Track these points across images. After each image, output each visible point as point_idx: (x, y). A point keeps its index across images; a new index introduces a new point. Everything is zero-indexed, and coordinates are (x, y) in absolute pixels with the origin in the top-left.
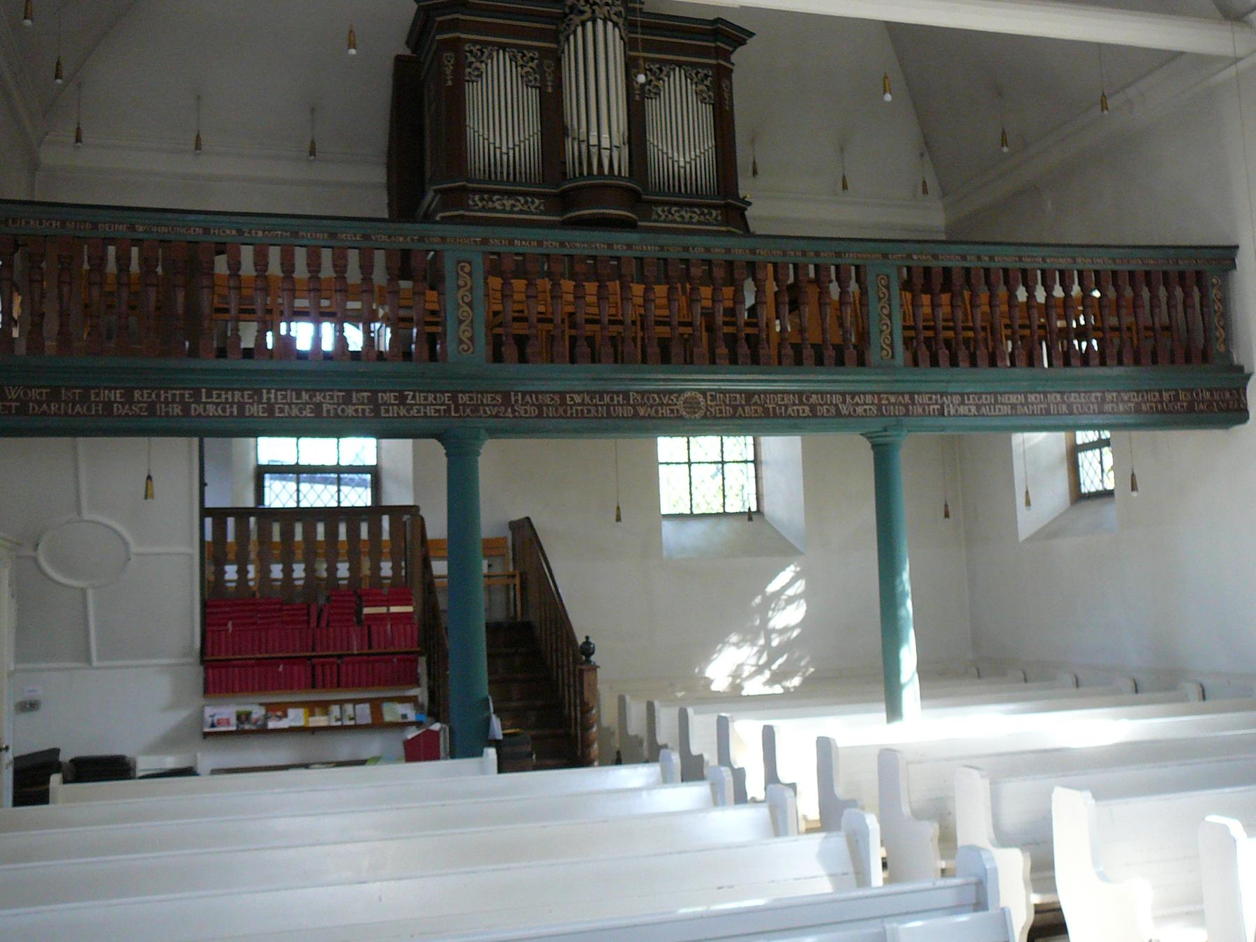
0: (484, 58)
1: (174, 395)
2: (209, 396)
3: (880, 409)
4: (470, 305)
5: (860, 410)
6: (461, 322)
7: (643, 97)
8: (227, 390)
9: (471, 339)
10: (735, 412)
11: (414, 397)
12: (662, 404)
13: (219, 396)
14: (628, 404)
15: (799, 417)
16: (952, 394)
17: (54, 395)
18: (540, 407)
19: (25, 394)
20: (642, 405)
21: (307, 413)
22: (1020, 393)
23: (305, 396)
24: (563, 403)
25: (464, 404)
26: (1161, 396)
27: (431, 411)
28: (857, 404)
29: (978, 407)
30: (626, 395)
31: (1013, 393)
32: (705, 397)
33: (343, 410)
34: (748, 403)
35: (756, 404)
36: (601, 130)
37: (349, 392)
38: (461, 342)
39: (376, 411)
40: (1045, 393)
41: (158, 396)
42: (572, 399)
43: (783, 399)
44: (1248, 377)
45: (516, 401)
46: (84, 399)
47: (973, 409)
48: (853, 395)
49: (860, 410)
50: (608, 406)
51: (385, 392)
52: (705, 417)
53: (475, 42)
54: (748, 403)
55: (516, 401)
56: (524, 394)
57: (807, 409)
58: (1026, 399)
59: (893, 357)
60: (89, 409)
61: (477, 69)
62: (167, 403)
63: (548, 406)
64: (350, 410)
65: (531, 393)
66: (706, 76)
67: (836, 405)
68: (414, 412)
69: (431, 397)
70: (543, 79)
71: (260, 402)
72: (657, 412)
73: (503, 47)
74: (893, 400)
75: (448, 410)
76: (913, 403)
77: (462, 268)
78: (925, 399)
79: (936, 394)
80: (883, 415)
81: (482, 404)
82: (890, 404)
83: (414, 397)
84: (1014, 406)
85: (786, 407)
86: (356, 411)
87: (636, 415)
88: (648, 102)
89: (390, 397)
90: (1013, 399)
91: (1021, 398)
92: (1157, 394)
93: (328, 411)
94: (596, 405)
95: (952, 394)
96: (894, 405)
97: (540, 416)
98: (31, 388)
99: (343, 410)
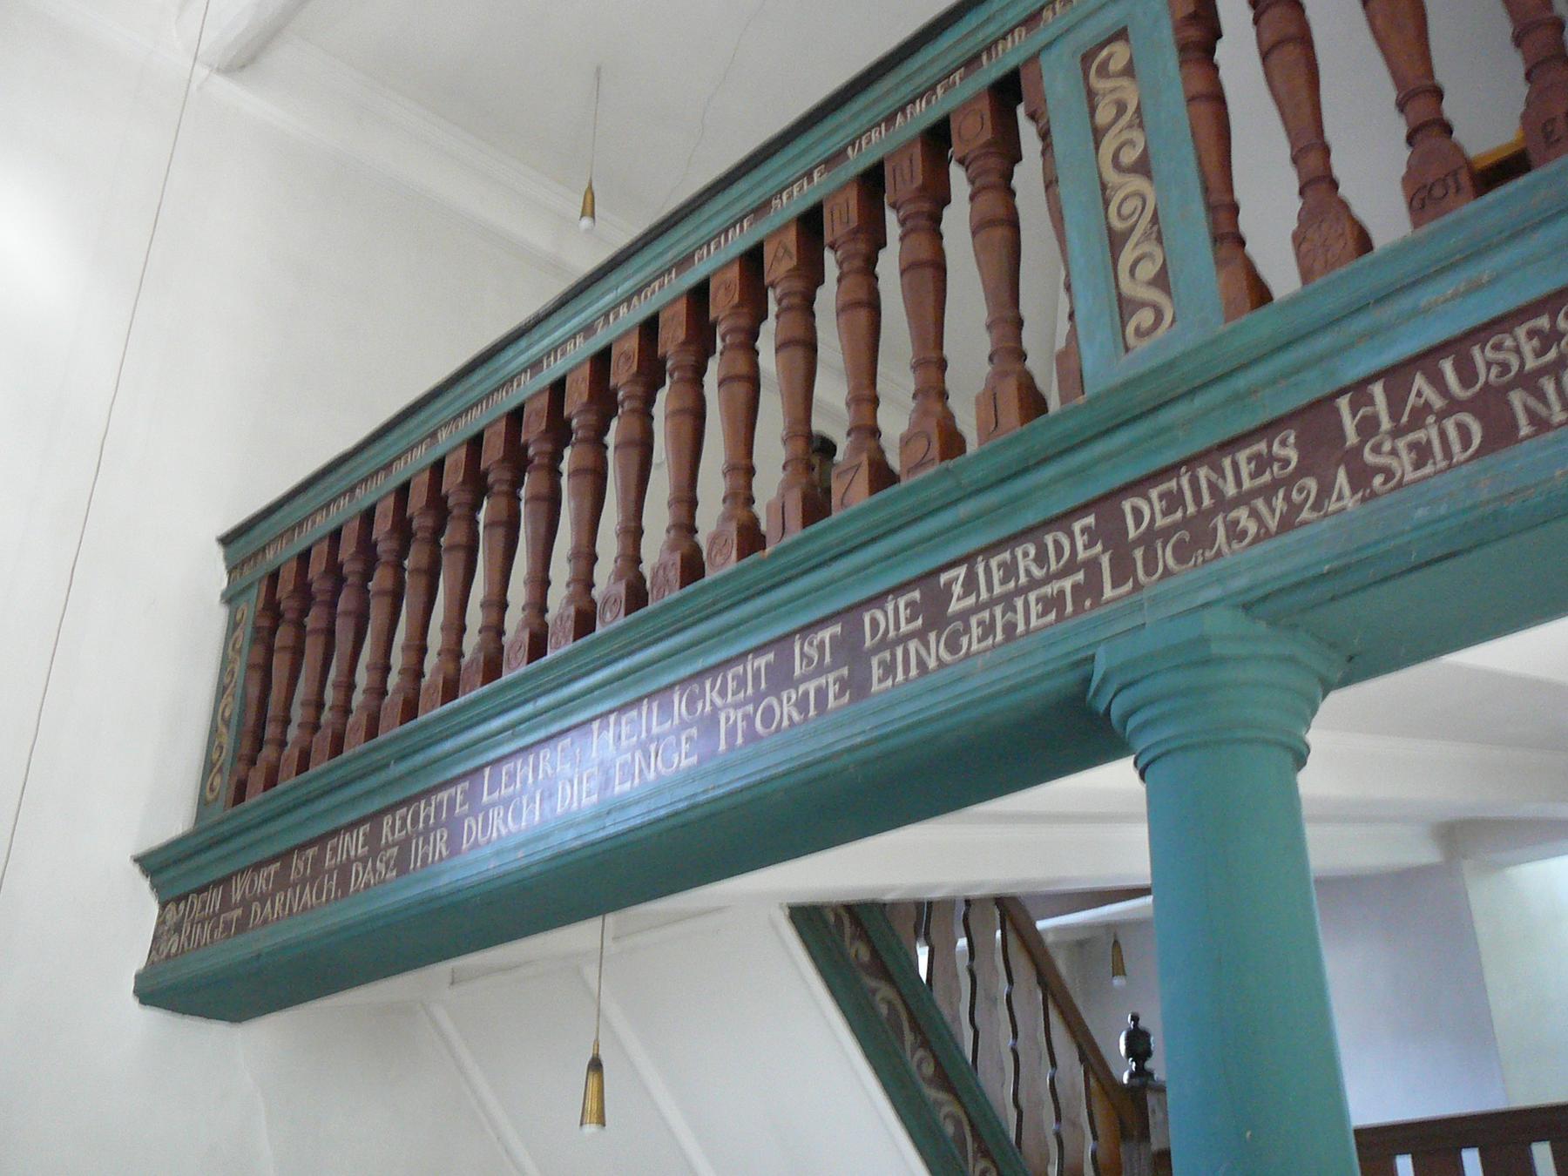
4: (1143, 167)
6: (1116, 242)
9: (1161, 280)
11: (970, 585)
25: (1150, 538)
33: (769, 714)
38: (1125, 307)
45: (1368, 427)
55: (1368, 427)
56: (1396, 375)
63: (1529, 381)
65: (1426, 360)
68: (972, 642)
75: (1089, 589)
77: (1103, 71)
81: (1223, 504)
83: (970, 585)
86: (802, 705)
89: (895, 616)
99: (769, 714)
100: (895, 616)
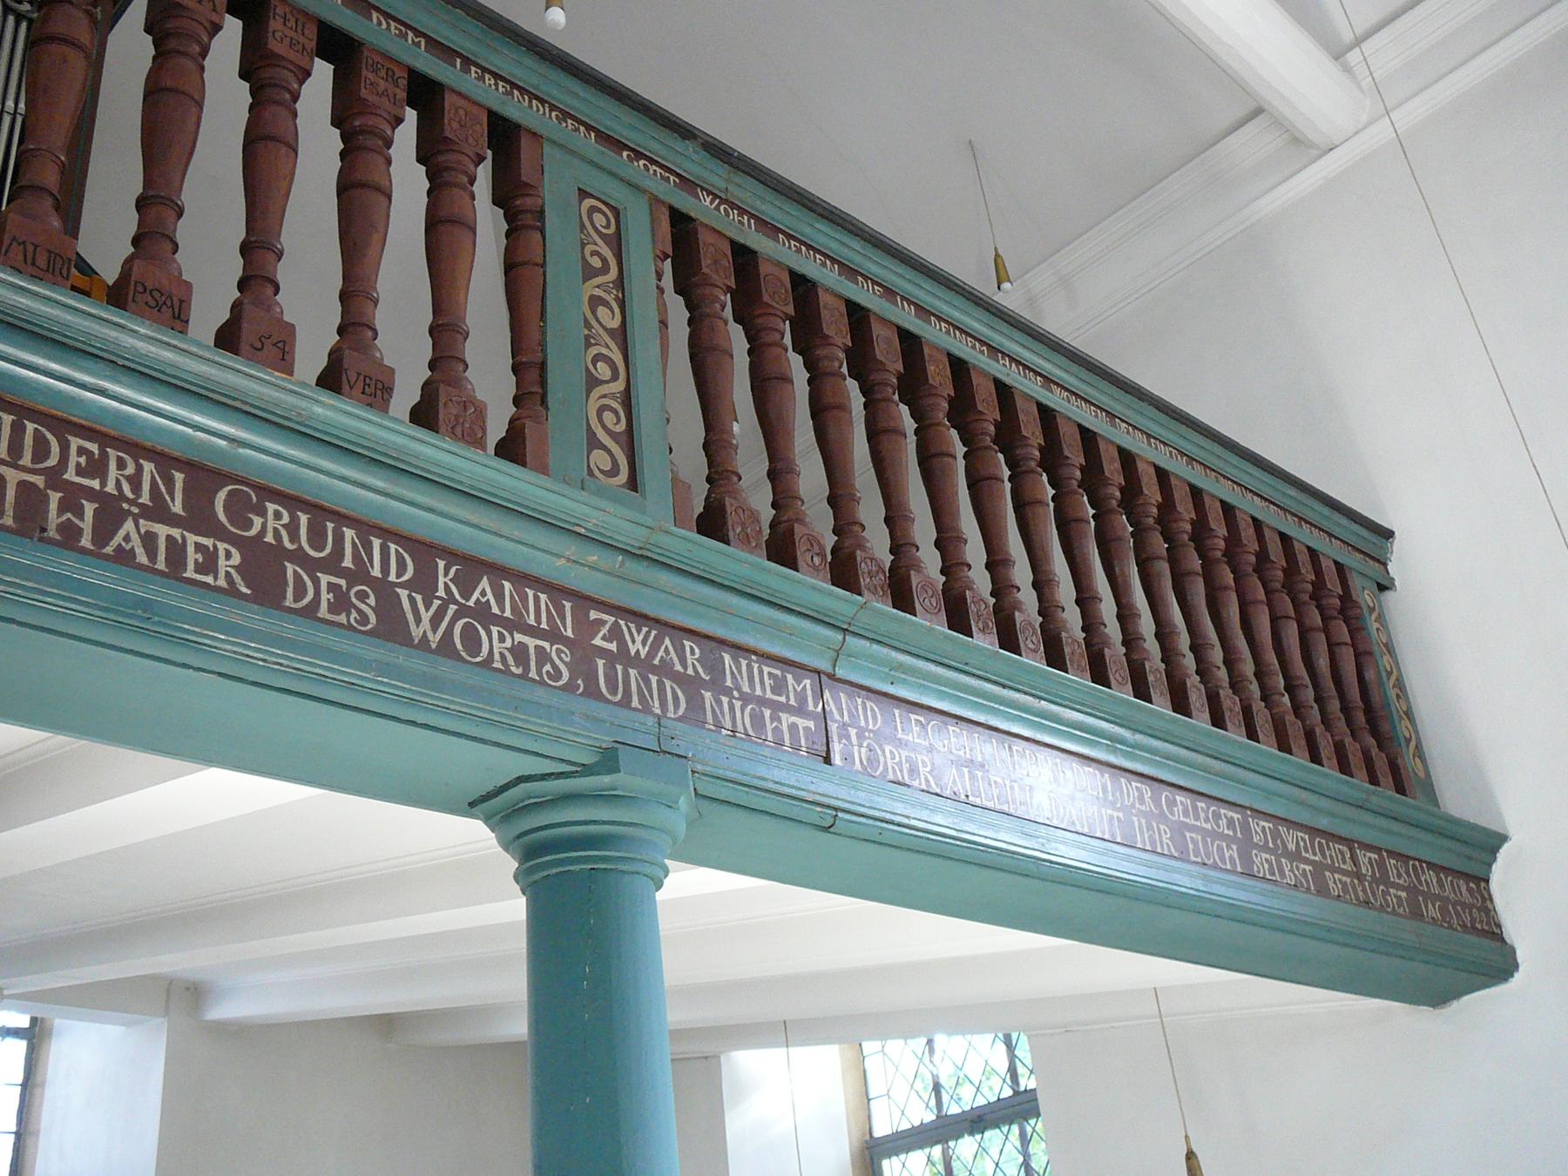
5: (495, 643)
28: (482, 613)
43: (96, 467)
44: (1490, 843)
48: (472, 567)
49: (495, 643)
57: (229, 560)
67: (384, 590)
74: (638, 645)
80: (599, 696)
85: (111, 513)
96: (645, 666)
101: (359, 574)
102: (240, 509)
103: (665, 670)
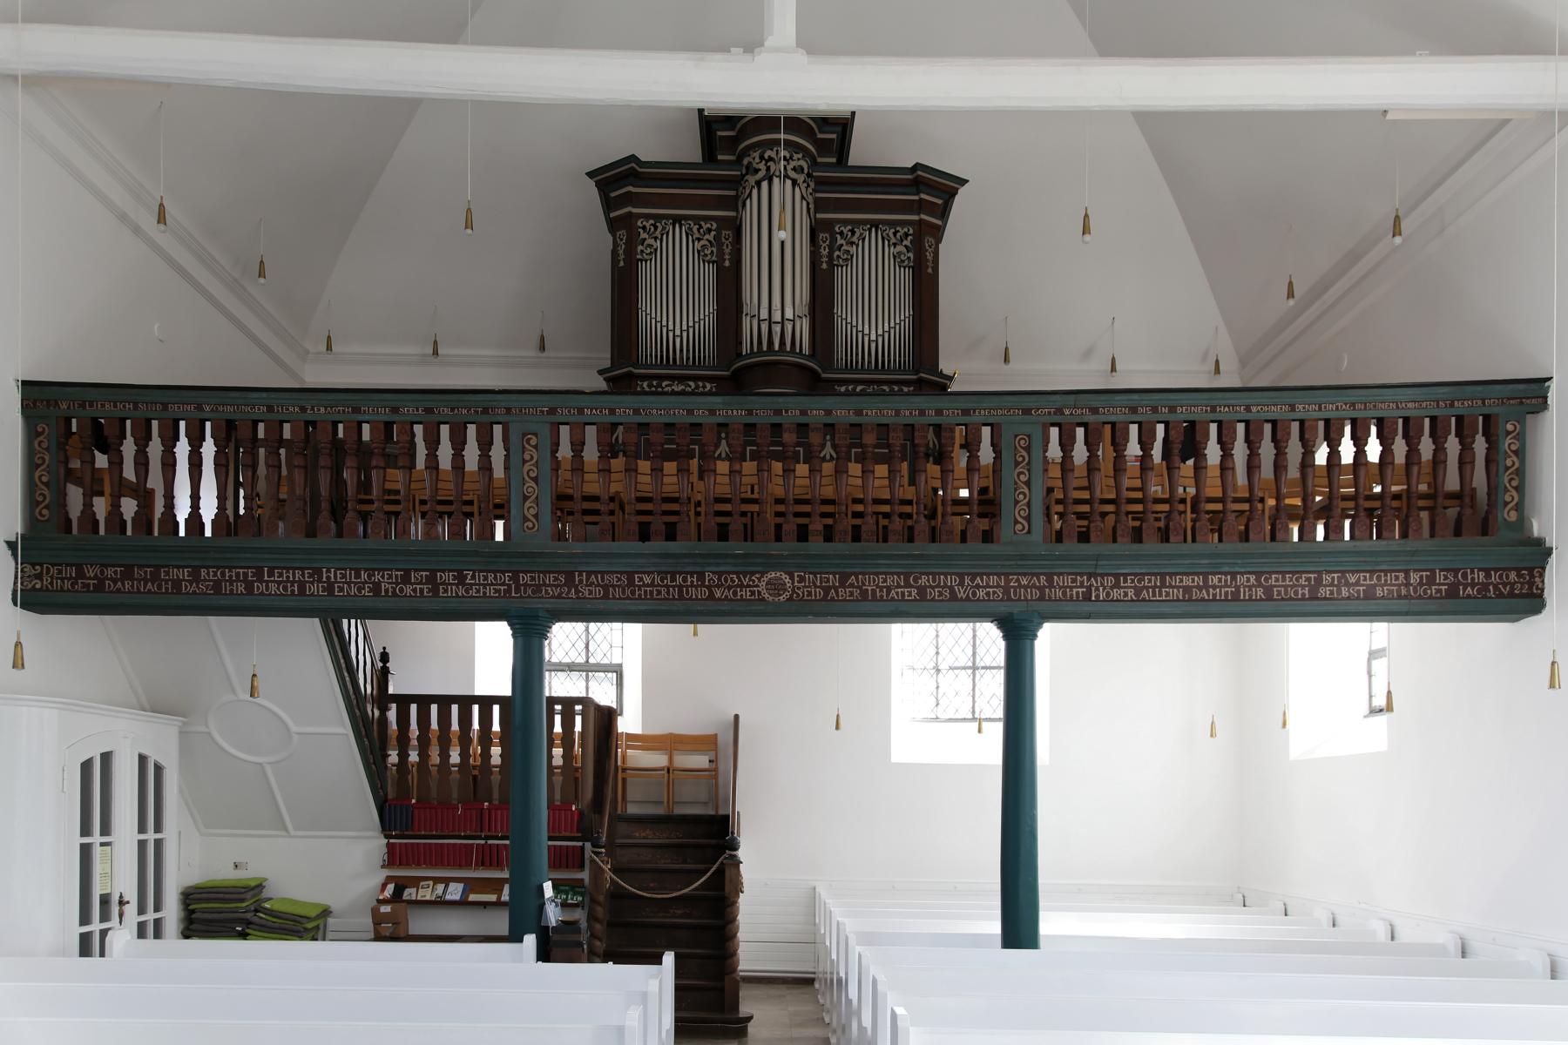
0: (658, 233)
1: (238, 574)
2: (271, 574)
3: (1006, 591)
5: (981, 593)
7: (832, 266)
8: (288, 569)
9: (536, 516)
10: (826, 594)
12: (741, 586)
13: (281, 575)
14: (703, 585)
15: (903, 600)
16: (1102, 575)
17: (128, 573)
18: (606, 588)
19: (102, 572)
20: (718, 586)
21: (366, 592)
22: (1198, 574)
23: (364, 576)
24: (631, 583)
25: (526, 585)
26: (1407, 577)
27: (490, 591)
28: (978, 586)
29: (1138, 591)
30: (701, 576)
31: (1187, 574)
32: (792, 578)
33: (401, 590)
34: (842, 585)
35: (852, 585)
36: (777, 301)
37: (407, 572)
38: (526, 519)
39: (435, 591)
40: (1234, 575)
41: (223, 574)
42: (641, 579)
45: (581, 581)
46: (155, 577)
47: (1131, 593)
50: (680, 587)
51: (443, 571)
52: (790, 599)
53: (647, 217)
54: (842, 585)
55: (581, 581)
56: (589, 574)
57: (914, 592)
58: (1206, 581)
59: (1029, 532)
60: (160, 587)
61: (650, 246)
62: (231, 582)
63: (614, 586)
64: (408, 590)
65: (596, 573)
66: (906, 235)
68: (473, 592)
69: (491, 577)
70: (721, 253)
71: (319, 581)
72: (735, 593)
73: (677, 220)
74: (1024, 582)
75: (508, 591)
76: (1051, 586)
78: (1068, 581)
79: (1081, 575)
81: (545, 584)
82: (1020, 586)
83: (473, 577)
84: (1187, 589)
85: (889, 589)
86: (414, 590)
87: (711, 597)
88: (838, 272)
89: (449, 577)
90: (1187, 581)
91: (1199, 580)
92: (1401, 576)
93: (387, 591)
94: (667, 586)
95: (1102, 575)
96: (1026, 587)
97: (606, 597)
98: (106, 566)
100: (449, 577)
101: (945, 586)
102: (916, 580)
103: (1034, 586)
